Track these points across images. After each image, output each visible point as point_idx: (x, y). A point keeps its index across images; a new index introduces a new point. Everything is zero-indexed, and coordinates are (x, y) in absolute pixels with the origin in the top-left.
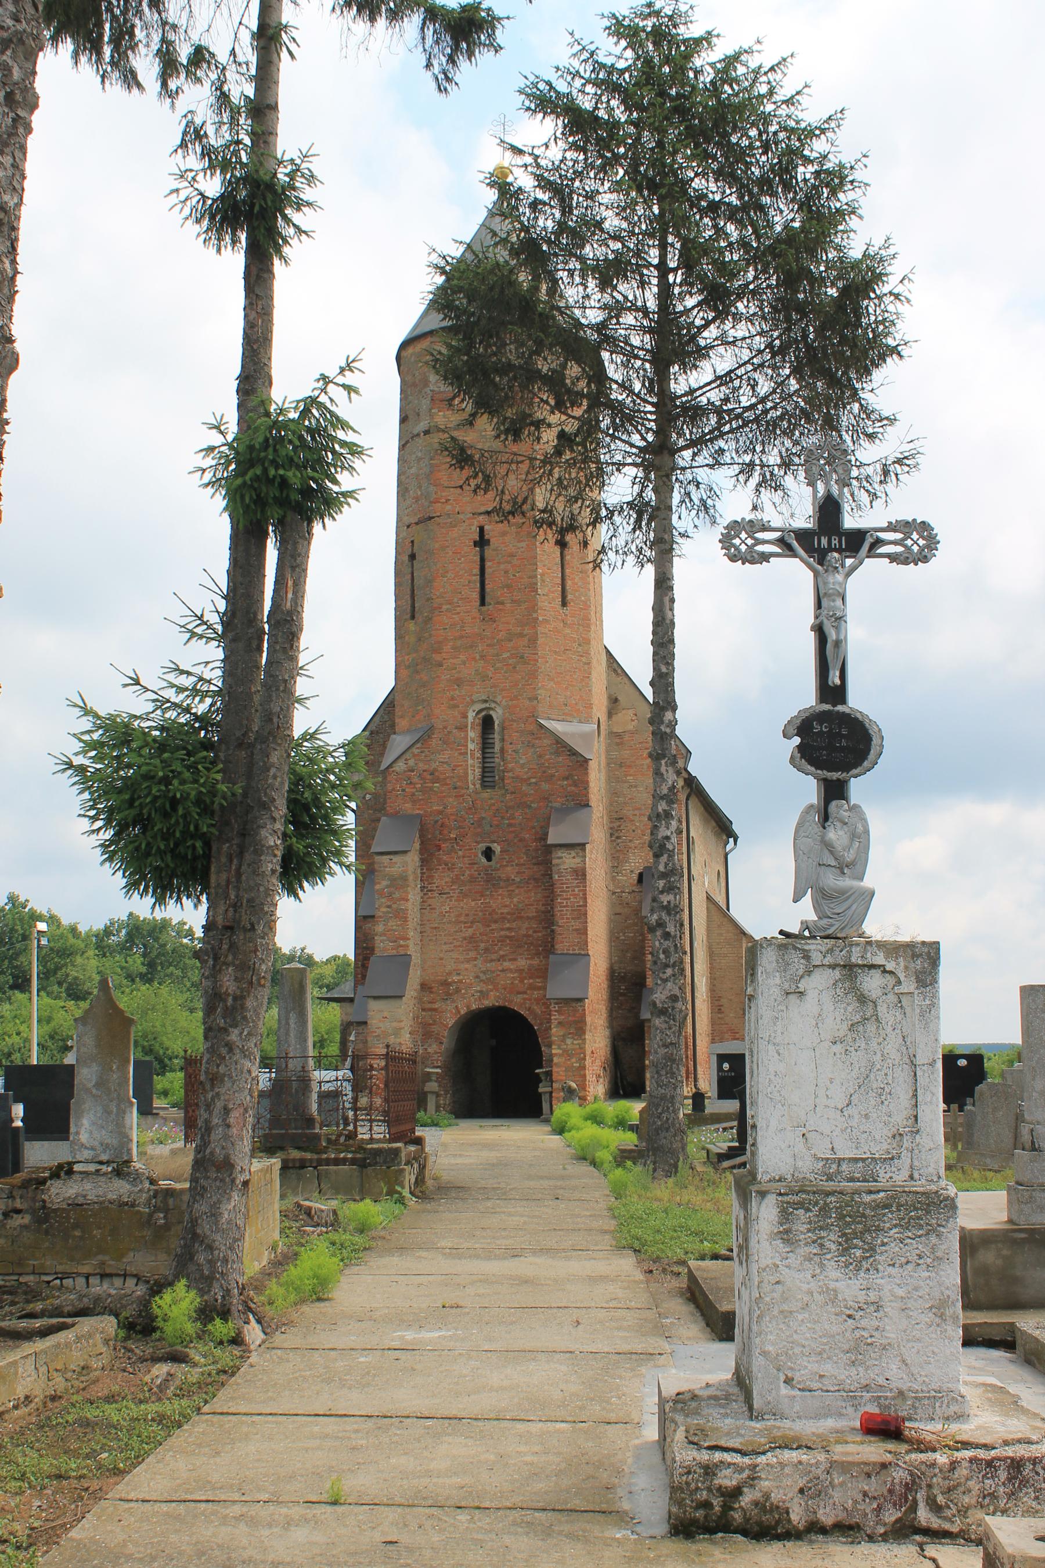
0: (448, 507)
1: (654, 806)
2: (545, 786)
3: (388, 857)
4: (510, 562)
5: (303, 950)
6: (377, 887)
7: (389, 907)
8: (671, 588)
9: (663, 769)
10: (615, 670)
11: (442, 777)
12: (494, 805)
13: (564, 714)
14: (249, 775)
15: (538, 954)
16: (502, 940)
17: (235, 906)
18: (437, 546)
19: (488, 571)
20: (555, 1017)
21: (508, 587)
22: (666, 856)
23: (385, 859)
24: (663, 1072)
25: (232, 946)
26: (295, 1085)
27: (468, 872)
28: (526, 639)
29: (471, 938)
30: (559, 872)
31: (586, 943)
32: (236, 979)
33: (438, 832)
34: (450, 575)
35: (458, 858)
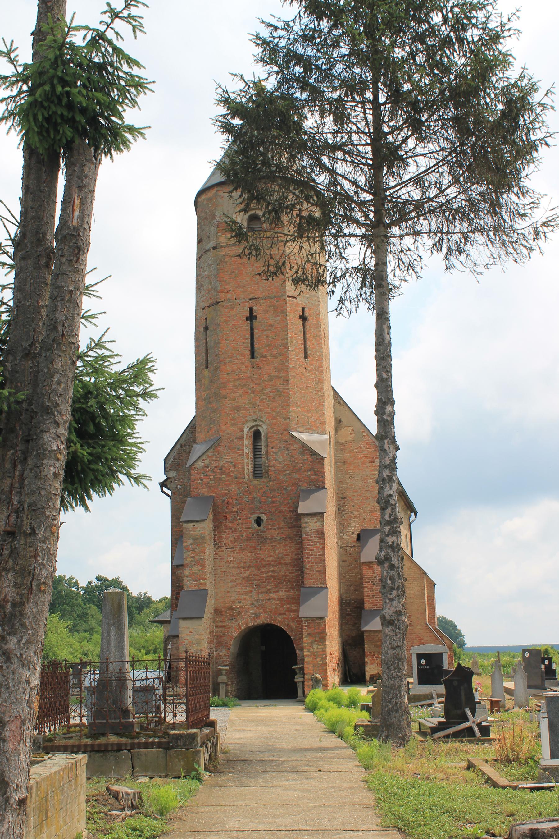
0: (229, 295)
1: (380, 473)
2: (295, 476)
3: (192, 524)
4: (270, 330)
5: (145, 594)
6: (185, 544)
7: (193, 557)
8: (388, 319)
9: (386, 446)
10: (339, 402)
11: (227, 471)
12: (261, 489)
13: (307, 428)
14: (35, 383)
15: (293, 588)
16: (268, 579)
17: (18, 511)
18: (222, 320)
19: (256, 336)
20: (305, 630)
21: (269, 346)
22: (390, 509)
23: (190, 525)
24: (392, 668)
25: (13, 551)
26: (114, 684)
27: (245, 534)
28: (282, 379)
29: (248, 578)
30: (306, 532)
31: (325, 579)
32: (16, 585)
33: (225, 508)
34: (230, 339)
35: (239, 524)
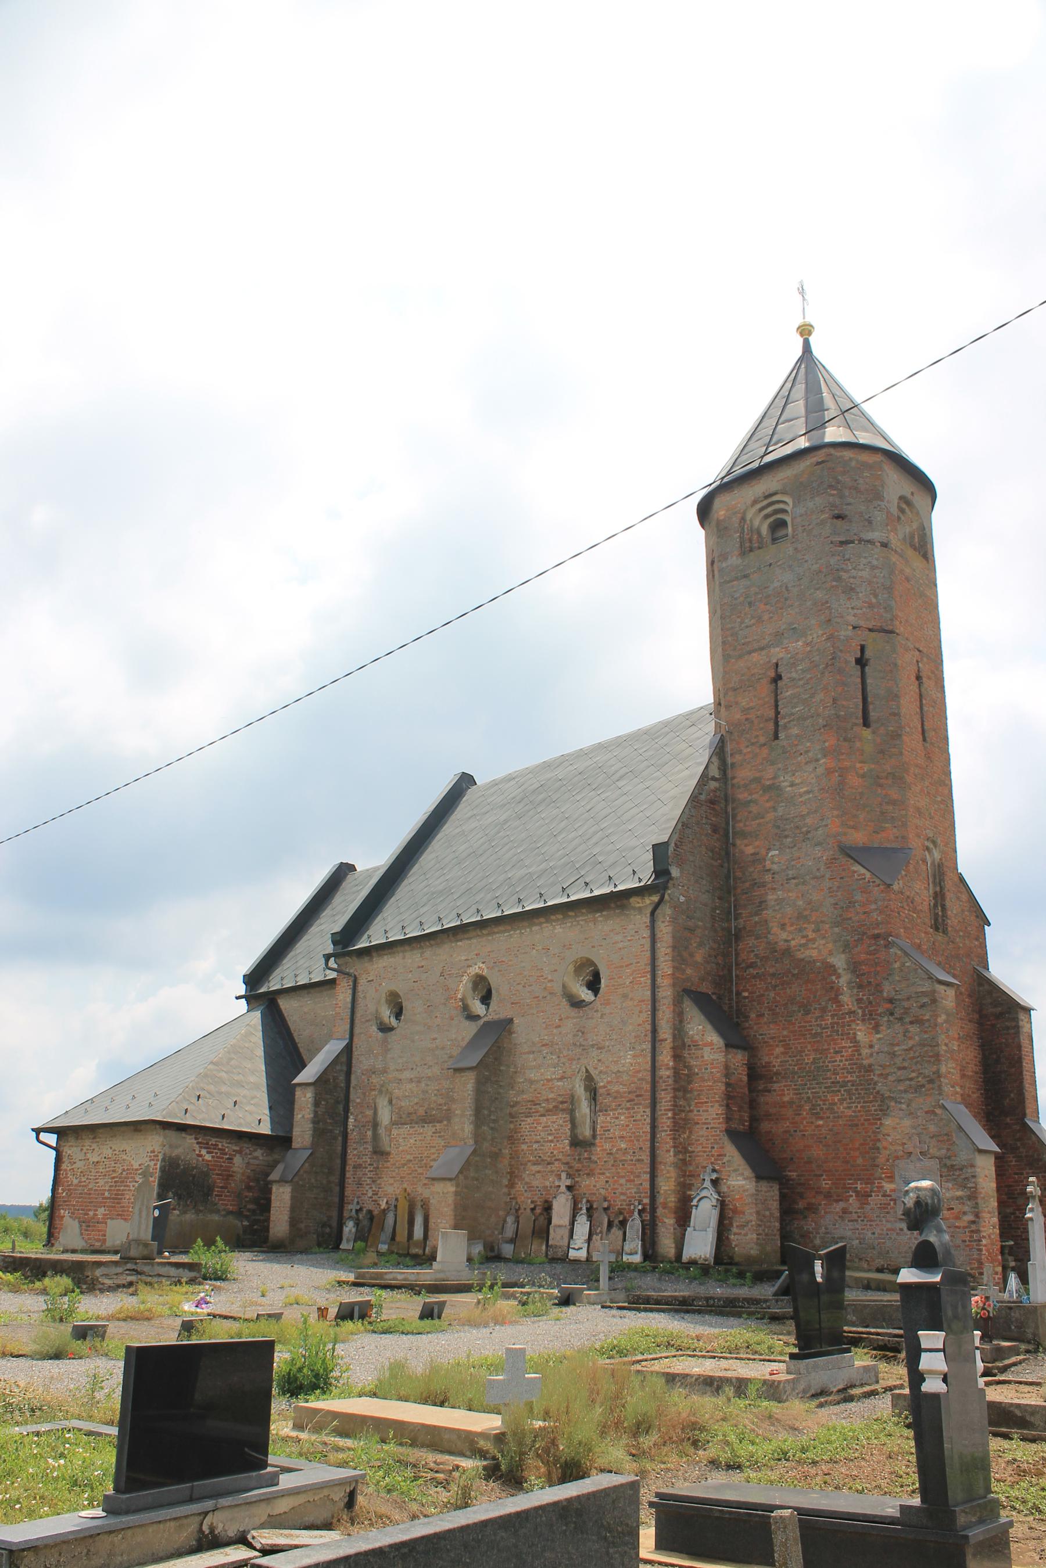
7: (946, 1045)
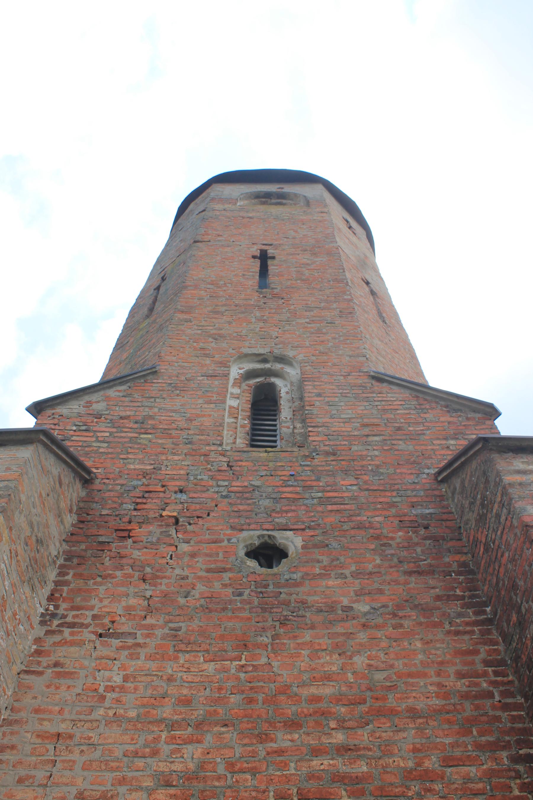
27: (200, 588)
